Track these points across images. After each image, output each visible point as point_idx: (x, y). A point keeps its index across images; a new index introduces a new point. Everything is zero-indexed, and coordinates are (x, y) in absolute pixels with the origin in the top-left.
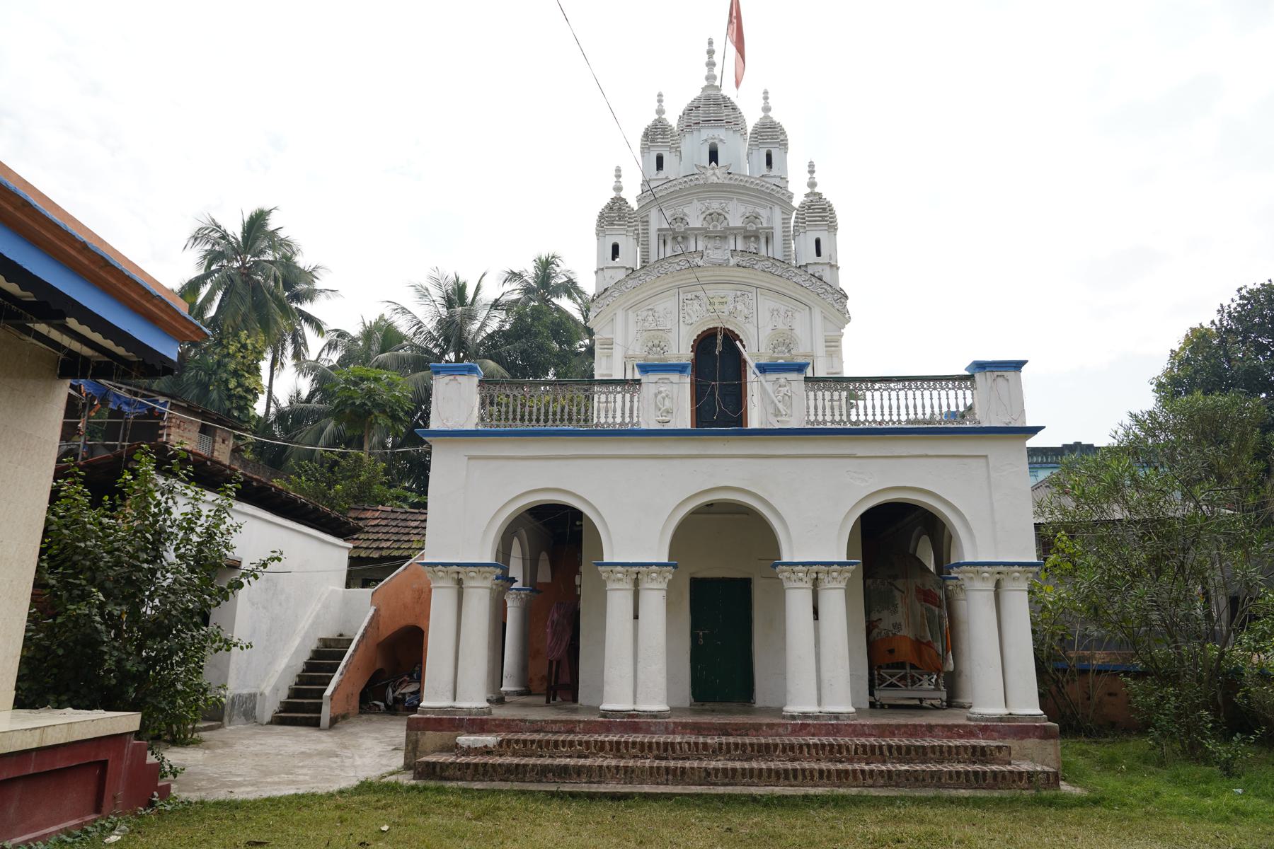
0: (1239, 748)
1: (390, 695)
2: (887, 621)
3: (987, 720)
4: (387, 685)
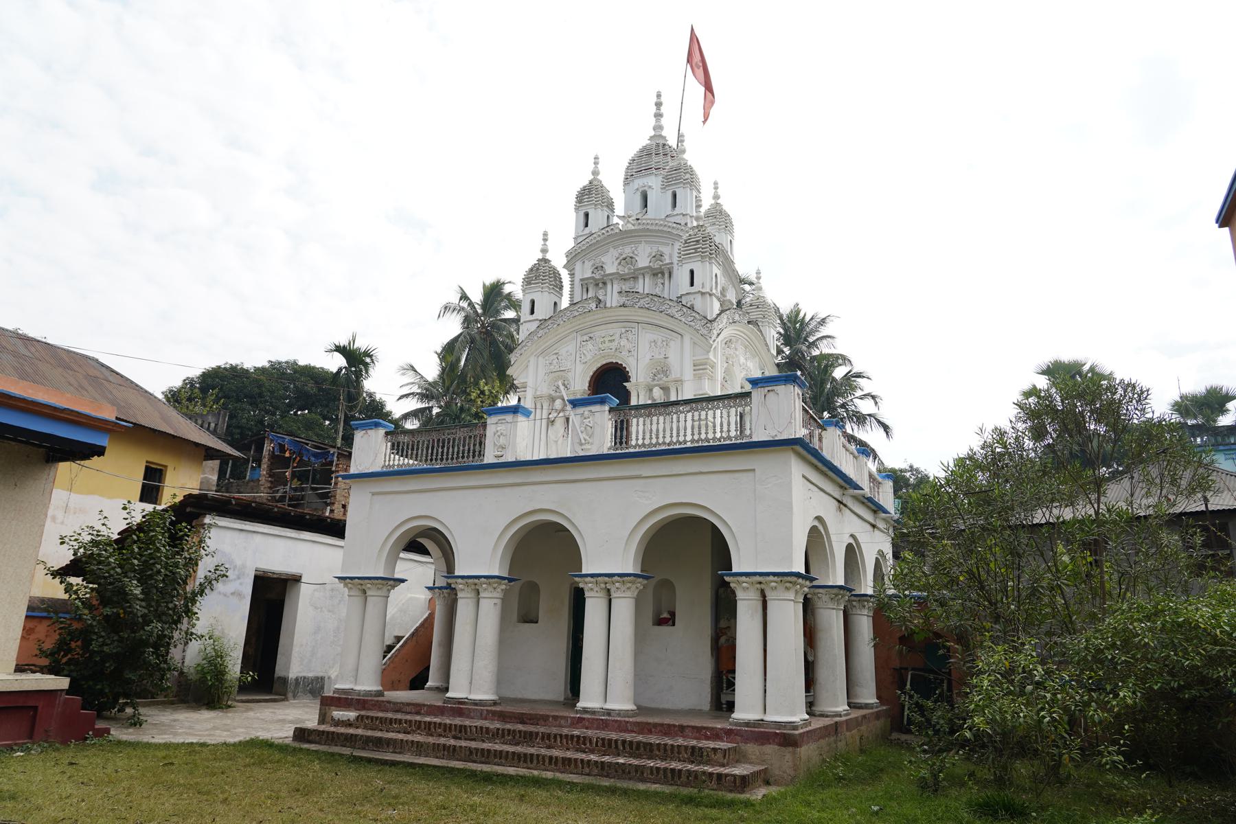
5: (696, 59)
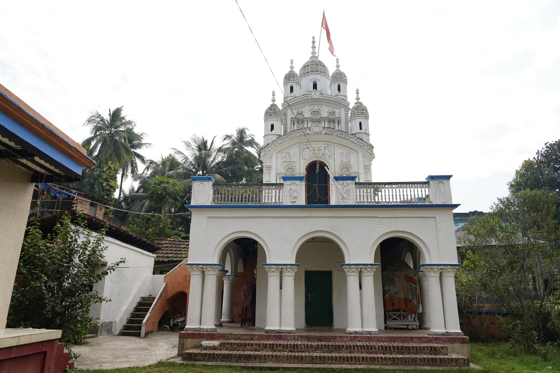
0: (549, 348)
1: (172, 323)
2: (393, 290)
3: (437, 335)
4: (170, 318)
5: (325, 25)
